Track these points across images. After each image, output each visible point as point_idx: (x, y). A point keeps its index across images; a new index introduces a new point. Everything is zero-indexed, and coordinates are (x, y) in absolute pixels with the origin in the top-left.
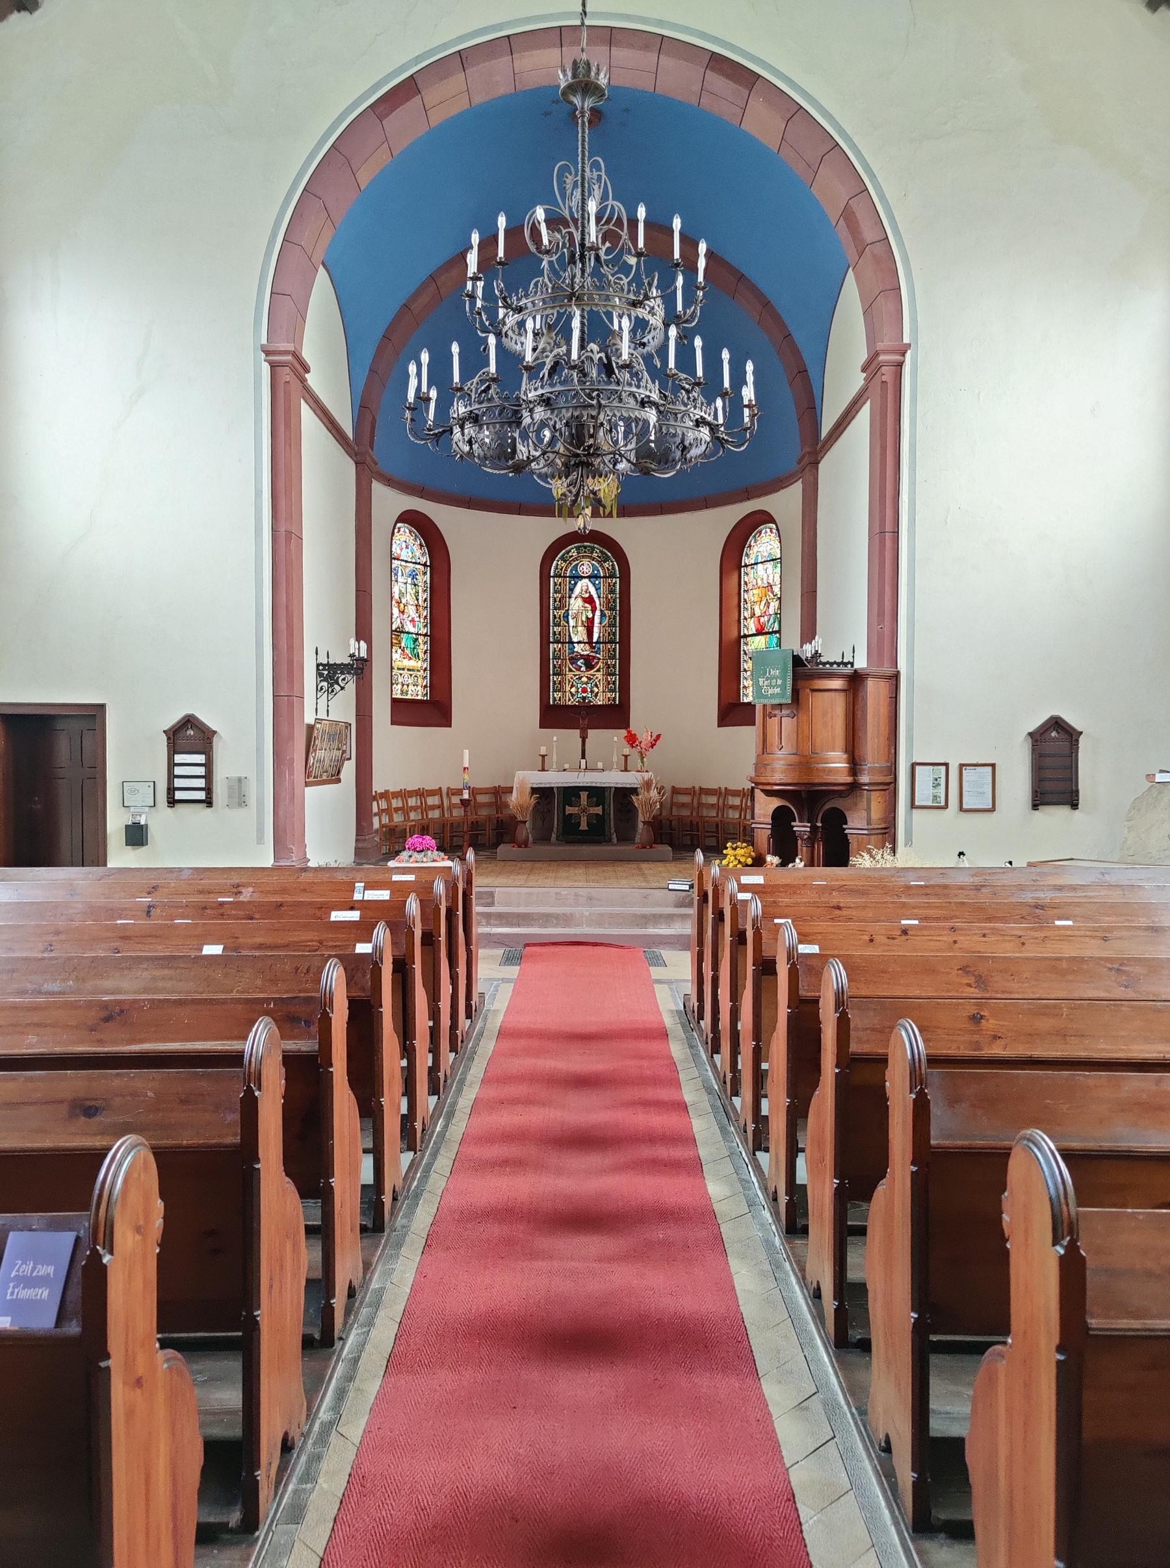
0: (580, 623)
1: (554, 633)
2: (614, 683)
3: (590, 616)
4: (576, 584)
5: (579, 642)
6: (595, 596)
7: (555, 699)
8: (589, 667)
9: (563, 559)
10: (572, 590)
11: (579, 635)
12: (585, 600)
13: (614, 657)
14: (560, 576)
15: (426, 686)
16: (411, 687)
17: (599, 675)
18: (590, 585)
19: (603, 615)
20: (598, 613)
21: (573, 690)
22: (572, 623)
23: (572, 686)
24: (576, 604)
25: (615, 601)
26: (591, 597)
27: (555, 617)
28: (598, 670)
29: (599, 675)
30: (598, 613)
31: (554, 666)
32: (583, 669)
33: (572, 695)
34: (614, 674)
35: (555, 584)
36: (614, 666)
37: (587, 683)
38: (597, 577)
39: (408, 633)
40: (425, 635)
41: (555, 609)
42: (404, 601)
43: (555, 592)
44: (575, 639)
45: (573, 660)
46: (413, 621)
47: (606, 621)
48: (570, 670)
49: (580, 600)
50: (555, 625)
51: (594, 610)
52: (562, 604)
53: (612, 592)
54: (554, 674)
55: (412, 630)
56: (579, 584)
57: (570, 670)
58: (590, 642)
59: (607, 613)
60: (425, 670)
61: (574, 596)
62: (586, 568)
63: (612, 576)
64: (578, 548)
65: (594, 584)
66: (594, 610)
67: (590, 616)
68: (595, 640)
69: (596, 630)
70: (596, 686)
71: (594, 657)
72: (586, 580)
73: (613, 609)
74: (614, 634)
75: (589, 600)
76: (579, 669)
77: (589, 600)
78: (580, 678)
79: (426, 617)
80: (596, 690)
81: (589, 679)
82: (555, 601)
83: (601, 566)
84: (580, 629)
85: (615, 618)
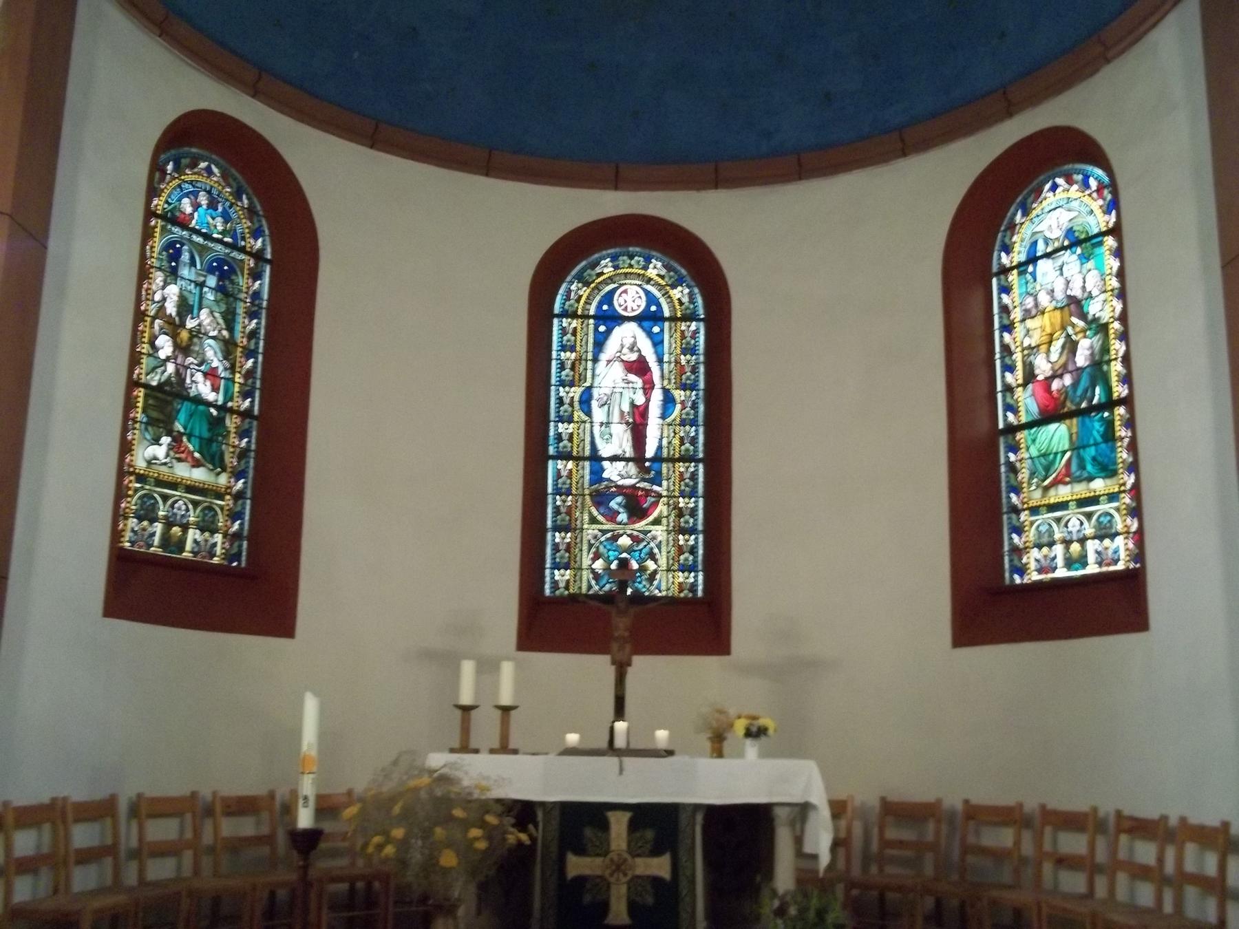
2: (693, 550)
8: (637, 509)
15: (237, 536)
16: (193, 534)
17: (659, 532)
28: (657, 522)
29: (659, 532)
32: (623, 517)
34: (692, 531)
37: (629, 550)
39: (198, 400)
40: (246, 414)
42: (190, 324)
46: (211, 374)
48: (593, 520)
55: (211, 397)
57: (593, 520)
60: (239, 496)
71: (648, 492)
76: (612, 516)
79: (249, 374)
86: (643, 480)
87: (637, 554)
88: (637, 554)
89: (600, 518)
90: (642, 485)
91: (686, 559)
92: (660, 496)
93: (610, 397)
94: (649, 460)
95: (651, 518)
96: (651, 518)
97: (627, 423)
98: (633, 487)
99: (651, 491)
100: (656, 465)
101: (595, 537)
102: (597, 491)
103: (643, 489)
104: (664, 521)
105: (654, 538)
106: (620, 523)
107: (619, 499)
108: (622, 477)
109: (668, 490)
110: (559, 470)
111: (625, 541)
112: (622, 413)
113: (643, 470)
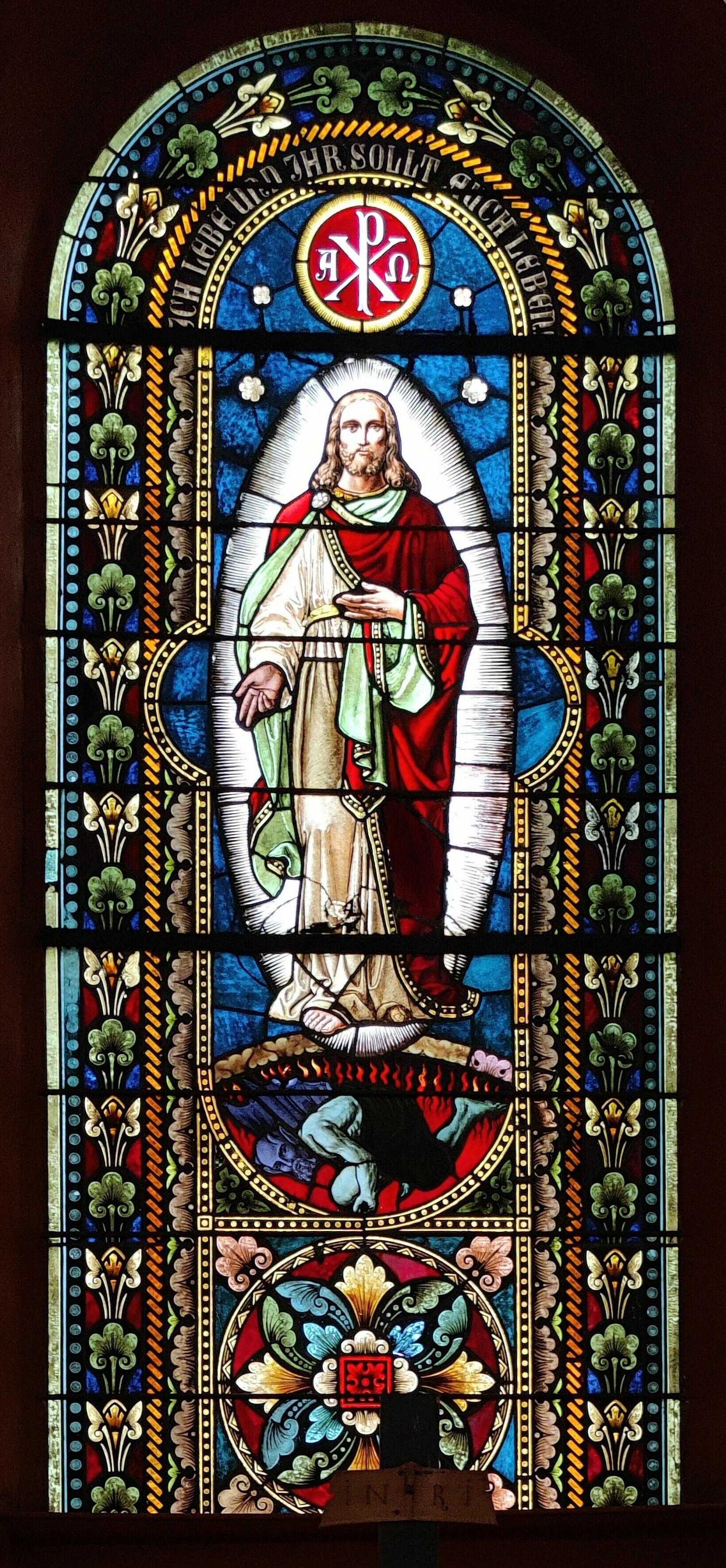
0: (319, 767)
1: (85, 855)
2: (640, 1313)
3: (414, 691)
4: (279, 404)
5: (310, 941)
6: (457, 513)
7: (88, 1462)
8: (408, 1156)
9: (152, 164)
10: (244, 460)
11: (317, 866)
12: (370, 554)
13: (633, 1079)
14: (130, 331)
18: (406, 407)
19: (526, 690)
20: (482, 669)
21: (260, 1378)
22: (246, 757)
23: (255, 1344)
24: (284, 589)
25: (637, 565)
26: (420, 516)
27: (86, 702)
28: (493, 1199)
30: (482, 669)
31: (87, 1161)
32: (353, 1183)
33: (254, 1423)
34: (639, 1234)
35: (90, 402)
36: (639, 1158)
37: (384, 1318)
38: (469, 342)
41: (91, 627)
43: (92, 474)
44: (278, 917)
45: (263, 1103)
47: (556, 741)
48: (236, 1198)
49: (313, 552)
50: (92, 778)
51: (446, 645)
52: (167, 593)
53: (616, 477)
54: (84, 1233)
56: (312, 410)
57: (236, 1198)
58: (412, 929)
59: (573, 668)
61: (262, 511)
62: (372, 249)
63: (616, 335)
64: (294, 71)
65: (446, 410)
66: (446, 645)
67: (414, 691)
68: (460, 910)
69: (468, 823)
70: (476, 1340)
71: (455, 1080)
72: (377, 374)
73: (622, 634)
74: (639, 862)
75: (405, 552)
77: (405, 552)
78: (325, 1271)
80: (472, 1377)
81: (408, 1278)
82: (89, 557)
83: (519, 239)
84: (320, 814)
85: (639, 717)
86: (432, 1028)
87: (415, 1330)
88: (415, 1330)
89: (262, 1186)
90: (430, 1048)
91: (614, 1351)
92: (502, 1092)
93: (290, 683)
94: (455, 944)
95: (467, 1187)
96: (467, 1187)
97: (364, 791)
98: (395, 1056)
99: (470, 1072)
100: (485, 971)
101: (246, 1266)
102: (248, 1074)
103: (434, 1065)
104: (522, 1195)
105: (481, 1267)
106: (346, 1209)
107: (339, 1108)
108: (350, 1020)
109: (535, 1070)
110: (87, 992)
111: (364, 1280)
112: (345, 745)
113: (436, 989)
